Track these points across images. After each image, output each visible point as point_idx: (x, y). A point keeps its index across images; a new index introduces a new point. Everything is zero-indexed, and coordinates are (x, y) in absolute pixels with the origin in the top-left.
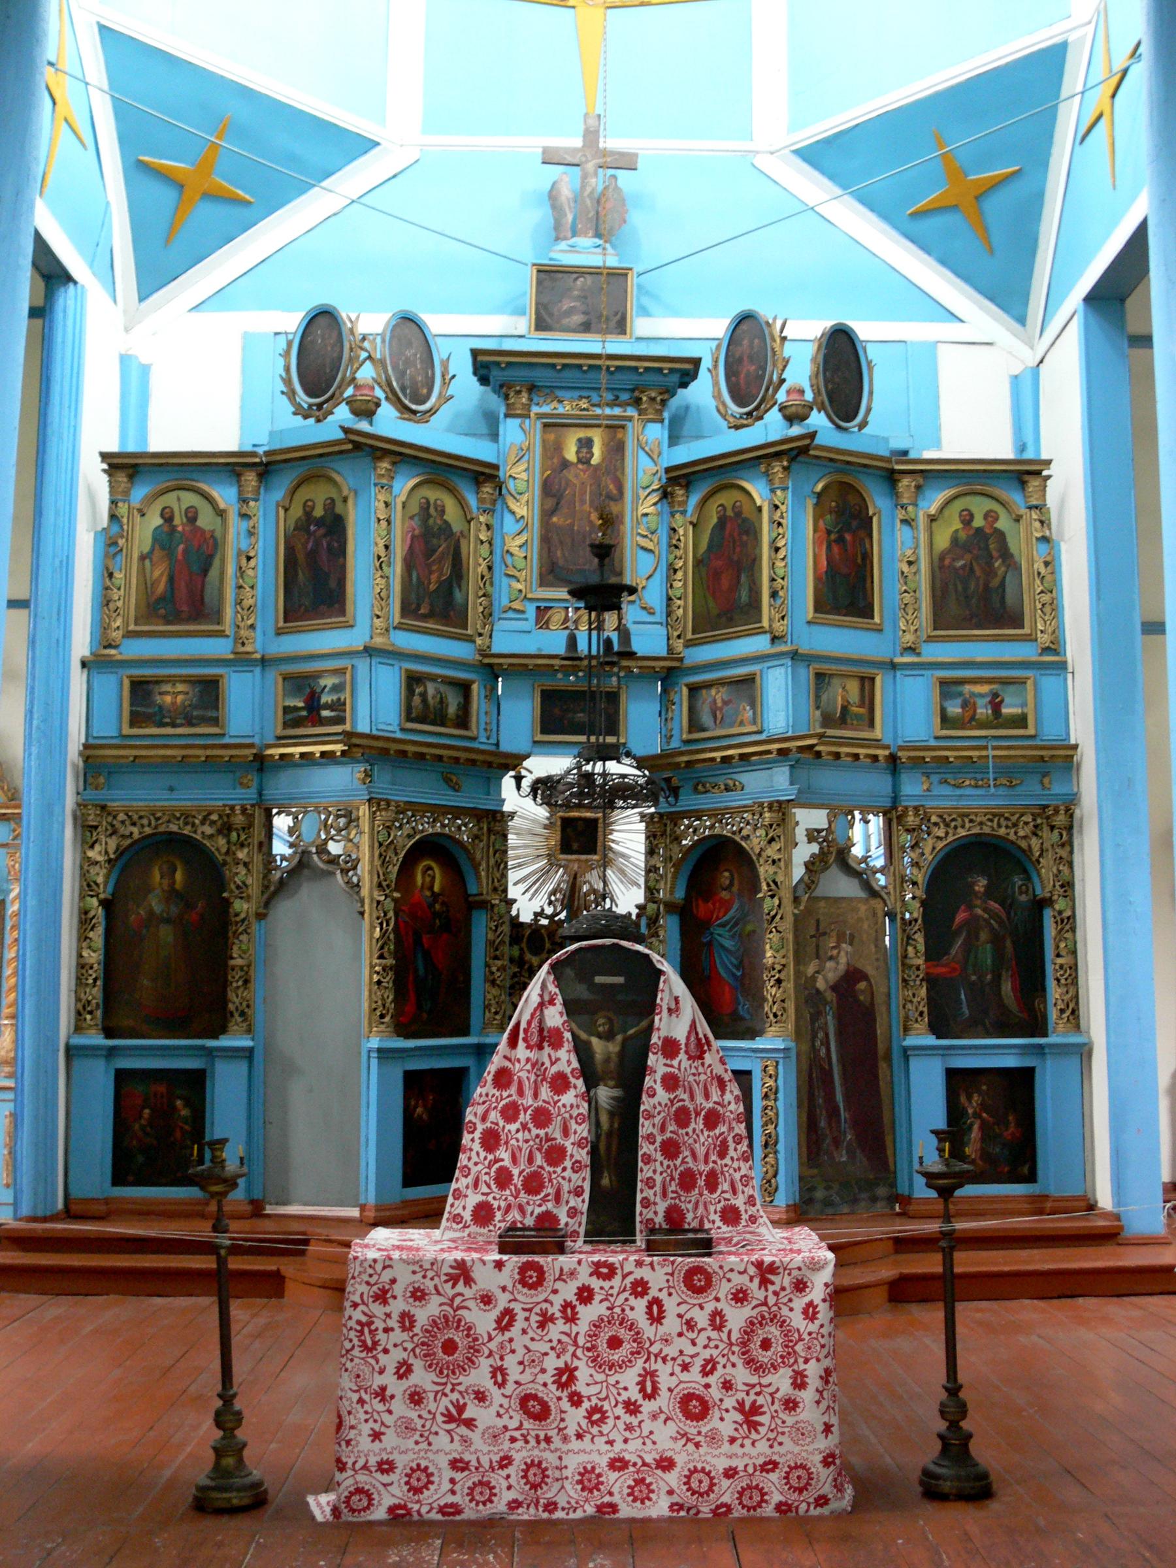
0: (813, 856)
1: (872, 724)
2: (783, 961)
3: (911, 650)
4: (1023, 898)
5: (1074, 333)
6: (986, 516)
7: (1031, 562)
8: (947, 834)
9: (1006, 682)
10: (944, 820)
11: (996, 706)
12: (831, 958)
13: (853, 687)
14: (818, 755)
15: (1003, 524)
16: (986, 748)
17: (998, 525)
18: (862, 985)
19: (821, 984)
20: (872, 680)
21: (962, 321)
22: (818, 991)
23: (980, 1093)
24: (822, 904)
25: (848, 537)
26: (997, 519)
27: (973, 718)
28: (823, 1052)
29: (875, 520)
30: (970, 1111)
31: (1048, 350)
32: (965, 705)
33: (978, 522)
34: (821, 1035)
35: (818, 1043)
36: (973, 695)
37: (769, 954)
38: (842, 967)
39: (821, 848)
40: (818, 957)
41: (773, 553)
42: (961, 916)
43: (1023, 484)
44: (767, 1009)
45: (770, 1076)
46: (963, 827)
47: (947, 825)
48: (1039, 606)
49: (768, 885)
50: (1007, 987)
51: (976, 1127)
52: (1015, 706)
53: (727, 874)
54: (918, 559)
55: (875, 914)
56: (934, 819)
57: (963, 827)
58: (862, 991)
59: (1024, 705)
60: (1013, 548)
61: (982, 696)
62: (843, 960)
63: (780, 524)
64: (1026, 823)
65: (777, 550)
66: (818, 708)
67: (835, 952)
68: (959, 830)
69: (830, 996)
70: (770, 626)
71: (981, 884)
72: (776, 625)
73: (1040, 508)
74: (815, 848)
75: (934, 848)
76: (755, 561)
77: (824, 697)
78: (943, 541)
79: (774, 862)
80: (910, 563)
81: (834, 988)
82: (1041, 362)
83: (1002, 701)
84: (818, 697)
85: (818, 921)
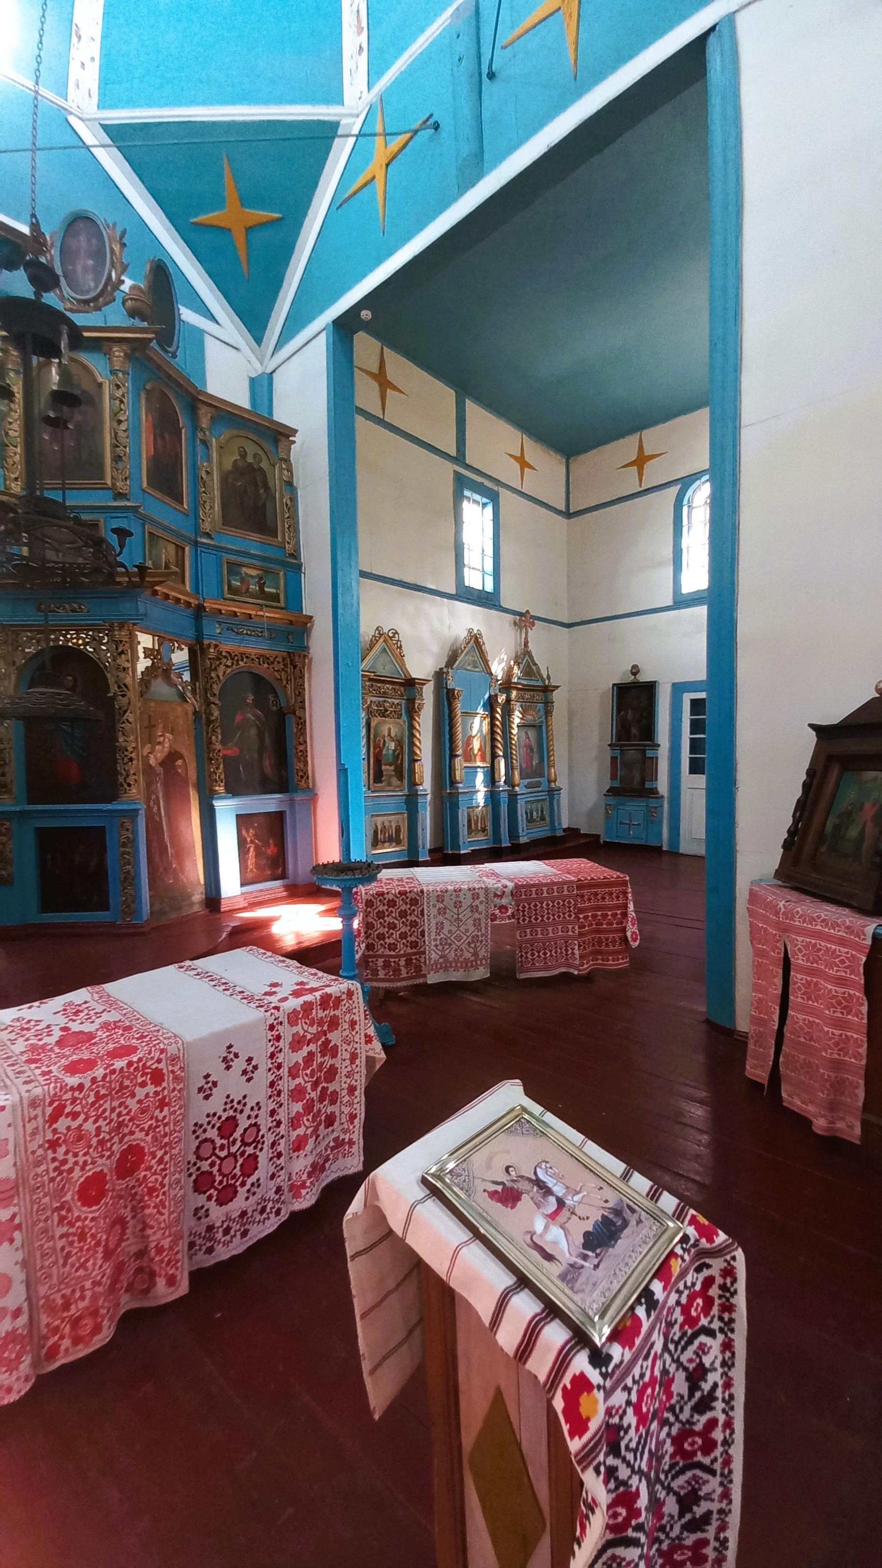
0: (147, 668)
1: (183, 582)
2: (134, 745)
3: (208, 535)
4: (275, 708)
5: (322, 342)
6: (255, 456)
7: (282, 497)
8: (233, 664)
9: (267, 571)
10: (231, 655)
11: (262, 587)
12: (159, 743)
13: (172, 549)
14: (155, 593)
15: (264, 465)
16: (261, 610)
17: (261, 465)
18: (179, 762)
19: (152, 762)
20: (183, 549)
21: (217, 323)
22: (150, 765)
23: (254, 828)
24: (152, 704)
25: (167, 436)
26: (261, 461)
27: (247, 590)
28: (155, 809)
29: (183, 431)
30: (249, 840)
31: (283, 363)
32: (242, 580)
33: (250, 459)
34: (153, 797)
35: (152, 803)
36: (246, 574)
37: (121, 740)
38: (166, 750)
39: (153, 663)
40: (150, 743)
41: (115, 424)
42: (238, 718)
43: (276, 442)
44: (121, 779)
45: (127, 830)
46: (242, 660)
47: (232, 659)
48: (287, 526)
49: (119, 687)
50: (266, 763)
51: (252, 849)
52: (273, 588)
53: (70, 678)
54: (212, 470)
55: (187, 714)
56: (224, 654)
57: (242, 660)
58: (180, 767)
59: (277, 588)
60: (271, 485)
61: (252, 577)
62: (167, 745)
63: (122, 402)
64: (279, 662)
65: (120, 422)
66: (150, 559)
67: (162, 739)
68: (240, 663)
69: (160, 770)
70: (113, 484)
71: (250, 699)
72: (119, 484)
73: (287, 461)
74: (149, 663)
75: (224, 673)
76: (98, 429)
77: (154, 552)
78: (228, 465)
79: (124, 669)
80: (208, 473)
81: (162, 764)
82: (274, 371)
83: (264, 583)
84: (150, 551)
85: (150, 717)
